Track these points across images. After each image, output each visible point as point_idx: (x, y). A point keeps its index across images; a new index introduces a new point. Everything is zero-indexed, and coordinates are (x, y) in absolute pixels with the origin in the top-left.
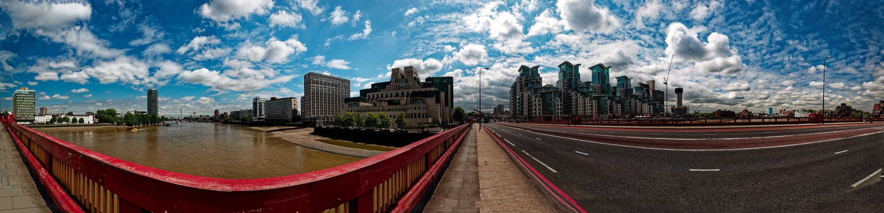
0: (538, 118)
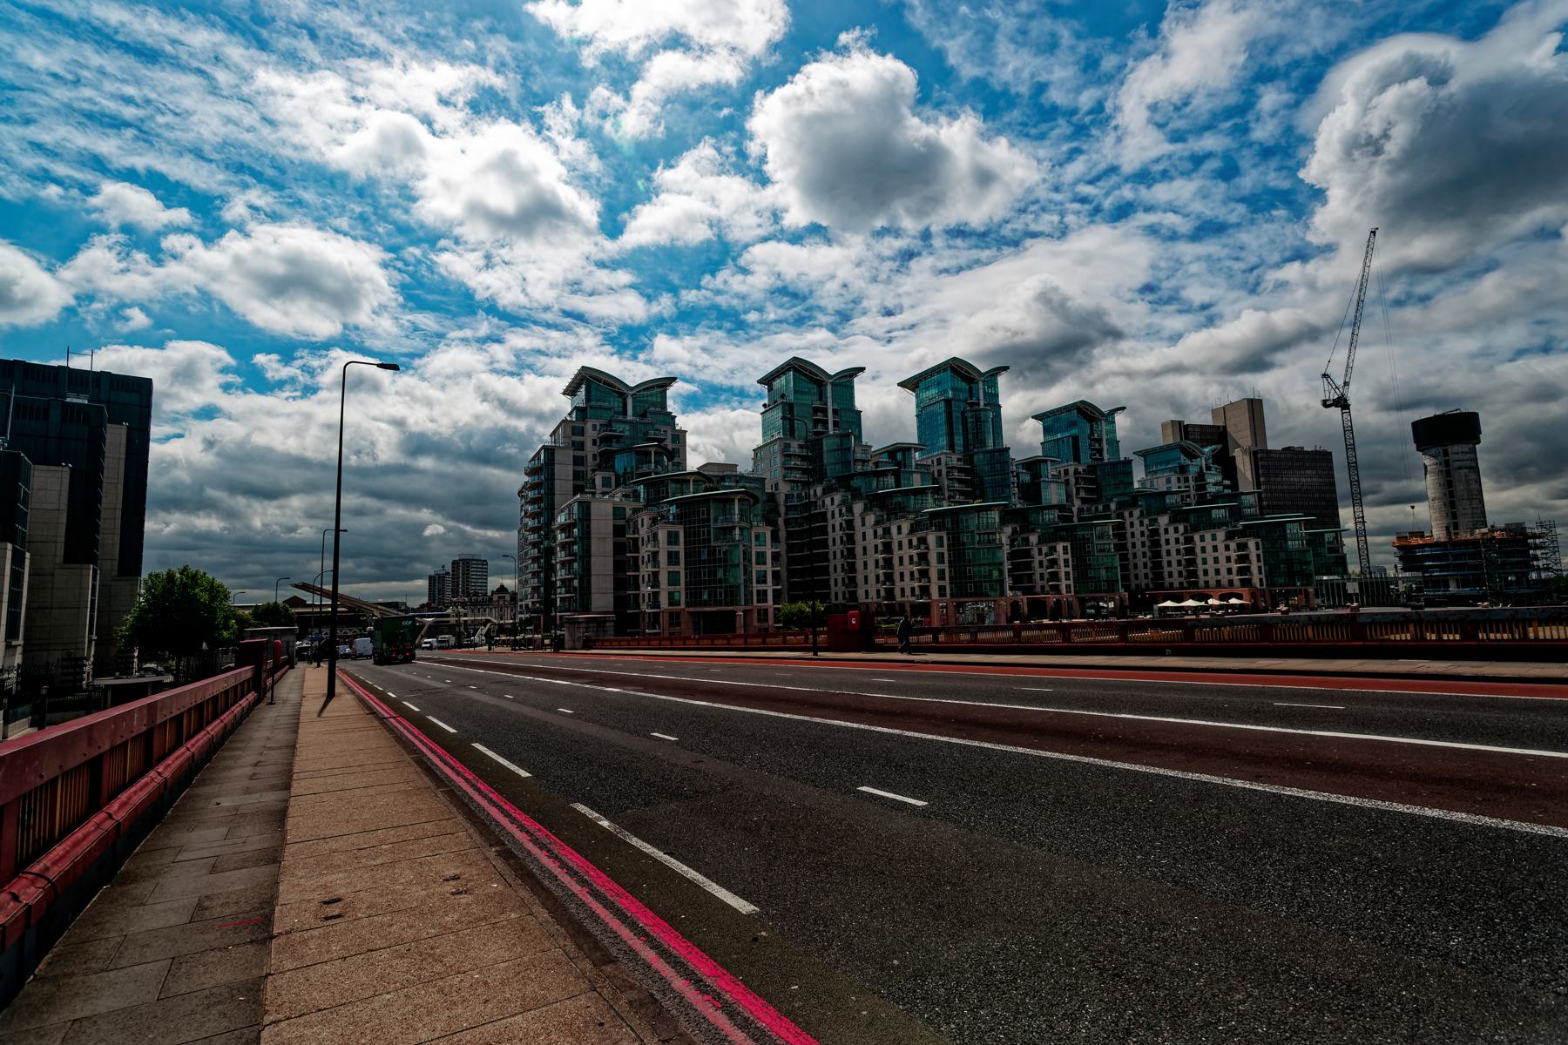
0: (664, 620)
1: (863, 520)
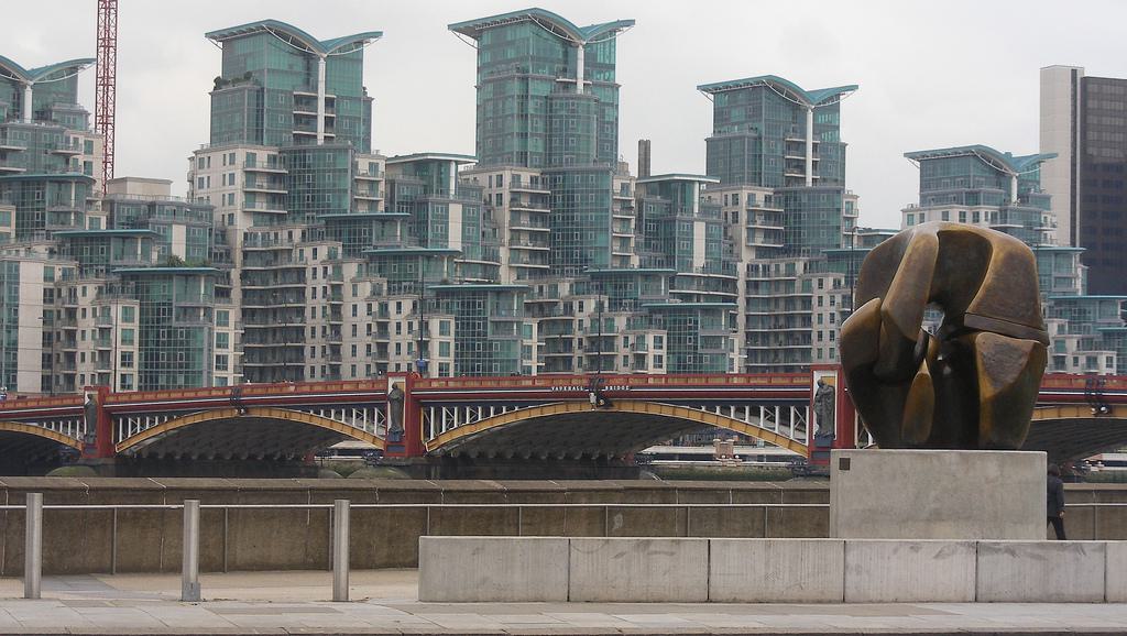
1: (355, 287)
